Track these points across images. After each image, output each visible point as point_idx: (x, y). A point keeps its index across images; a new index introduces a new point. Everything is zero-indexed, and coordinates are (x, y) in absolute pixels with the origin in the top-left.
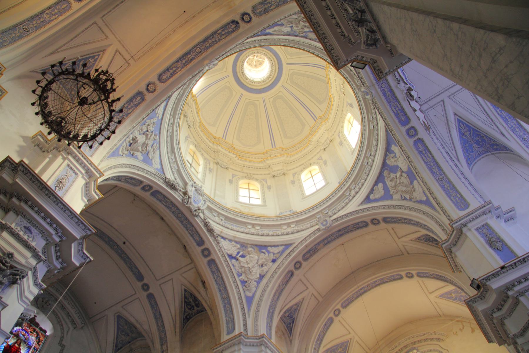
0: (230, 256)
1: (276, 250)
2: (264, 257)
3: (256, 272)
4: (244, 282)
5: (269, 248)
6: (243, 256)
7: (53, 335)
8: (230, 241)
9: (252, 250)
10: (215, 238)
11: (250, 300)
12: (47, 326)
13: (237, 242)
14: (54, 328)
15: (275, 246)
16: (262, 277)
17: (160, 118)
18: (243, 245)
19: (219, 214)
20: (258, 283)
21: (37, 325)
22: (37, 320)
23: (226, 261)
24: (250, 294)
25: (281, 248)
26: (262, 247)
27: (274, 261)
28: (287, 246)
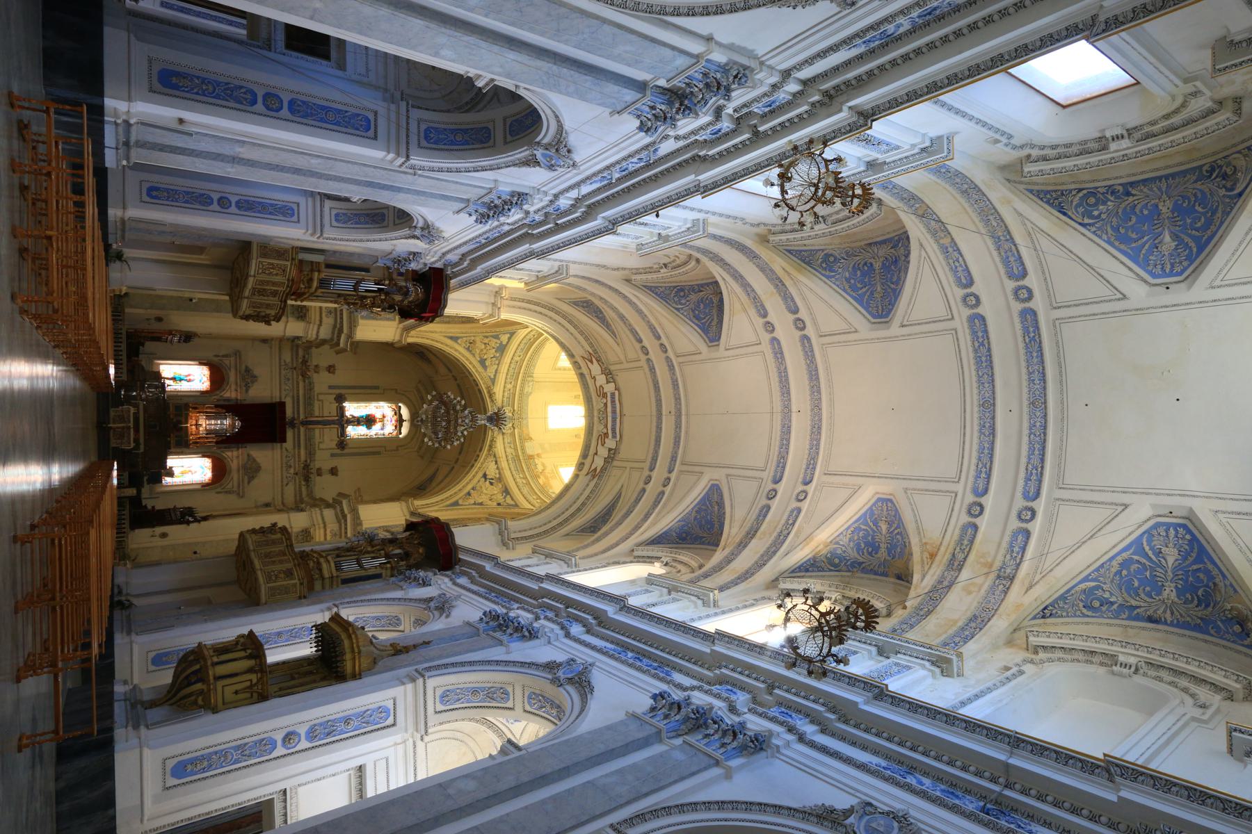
0: (485, 476)
1: (509, 500)
2: (500, 498)
3: (484, 499)
4: (469, 494)
5: (508, 498)
6: (491, 484)
7: (400, 439)
8: (498, 468)
9: (500, 485)
10: (489, 454)
11: (456, 504)
12: (405, 430)
13: (500, 473)
14: (406, 437)
15: (512, 499)
16: (481, 504)
17: (504, 343)
18: (500, 479)
19: (516, 449)
20: (475, 504)
21: (401, 426)
22: (404, 423)
23: (477, 473)
24: (460, 502)
25: (512, 503)
26: (506, 491)
27: (499, 504)
28: (516, 505)
